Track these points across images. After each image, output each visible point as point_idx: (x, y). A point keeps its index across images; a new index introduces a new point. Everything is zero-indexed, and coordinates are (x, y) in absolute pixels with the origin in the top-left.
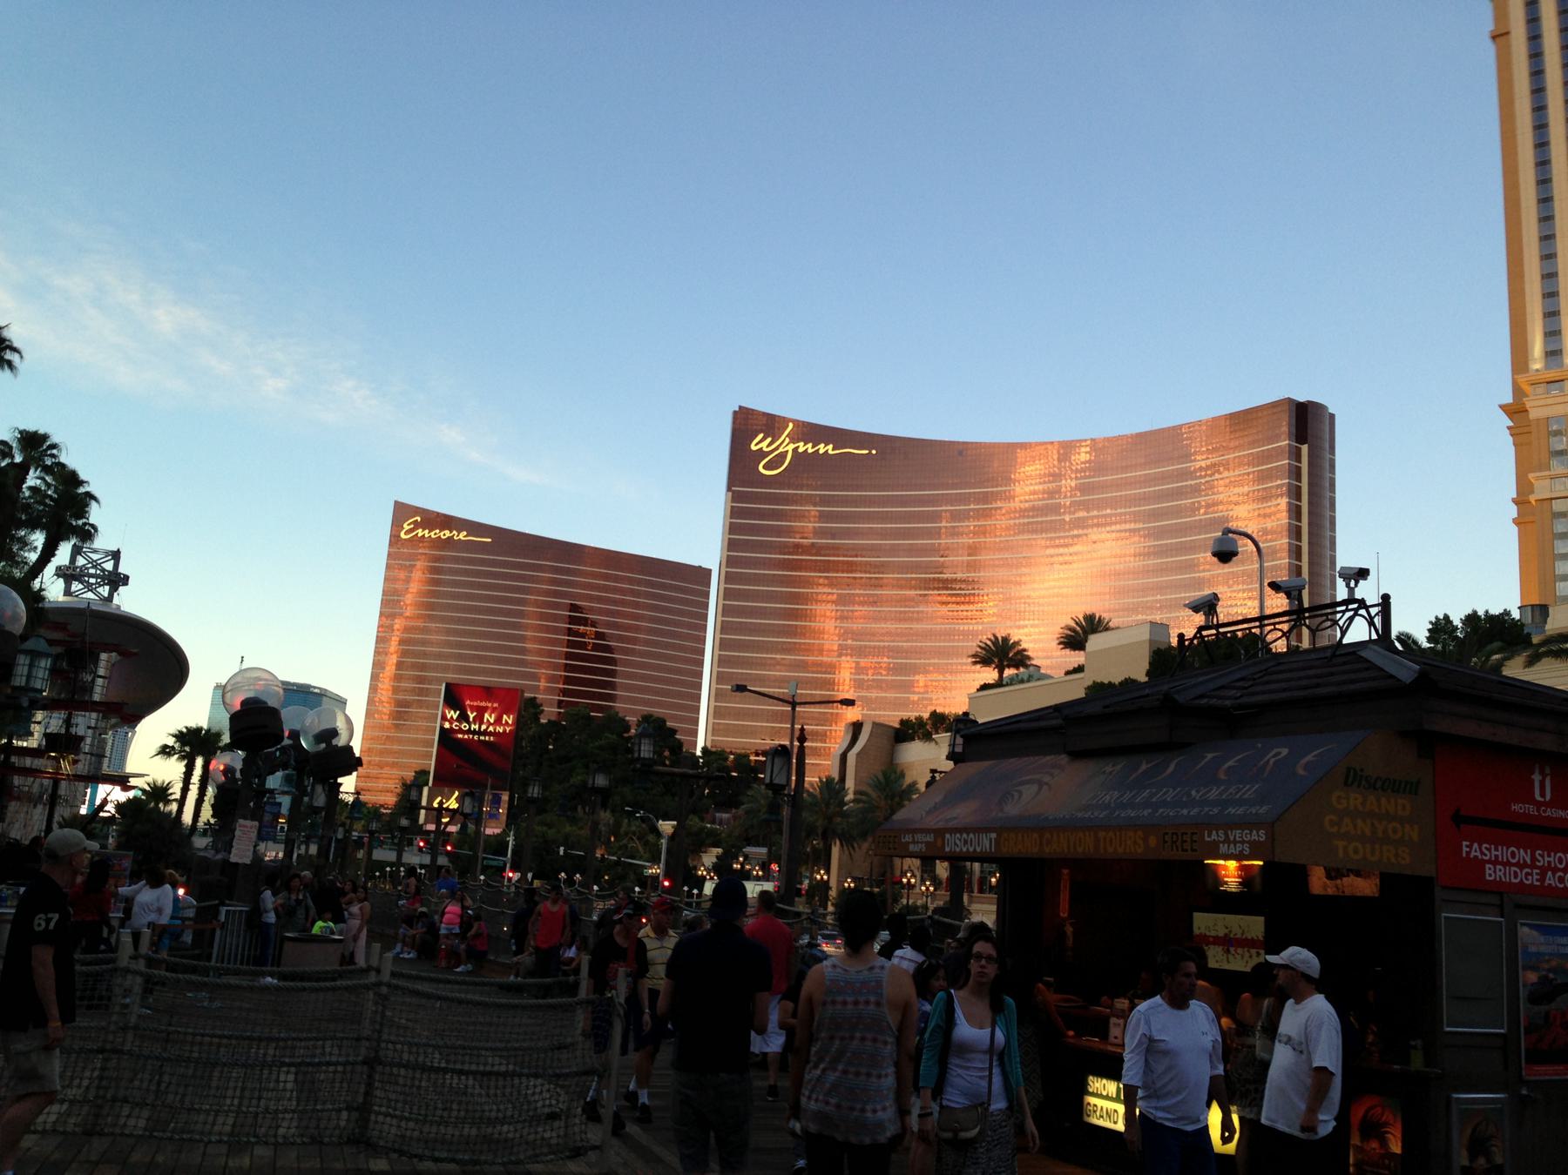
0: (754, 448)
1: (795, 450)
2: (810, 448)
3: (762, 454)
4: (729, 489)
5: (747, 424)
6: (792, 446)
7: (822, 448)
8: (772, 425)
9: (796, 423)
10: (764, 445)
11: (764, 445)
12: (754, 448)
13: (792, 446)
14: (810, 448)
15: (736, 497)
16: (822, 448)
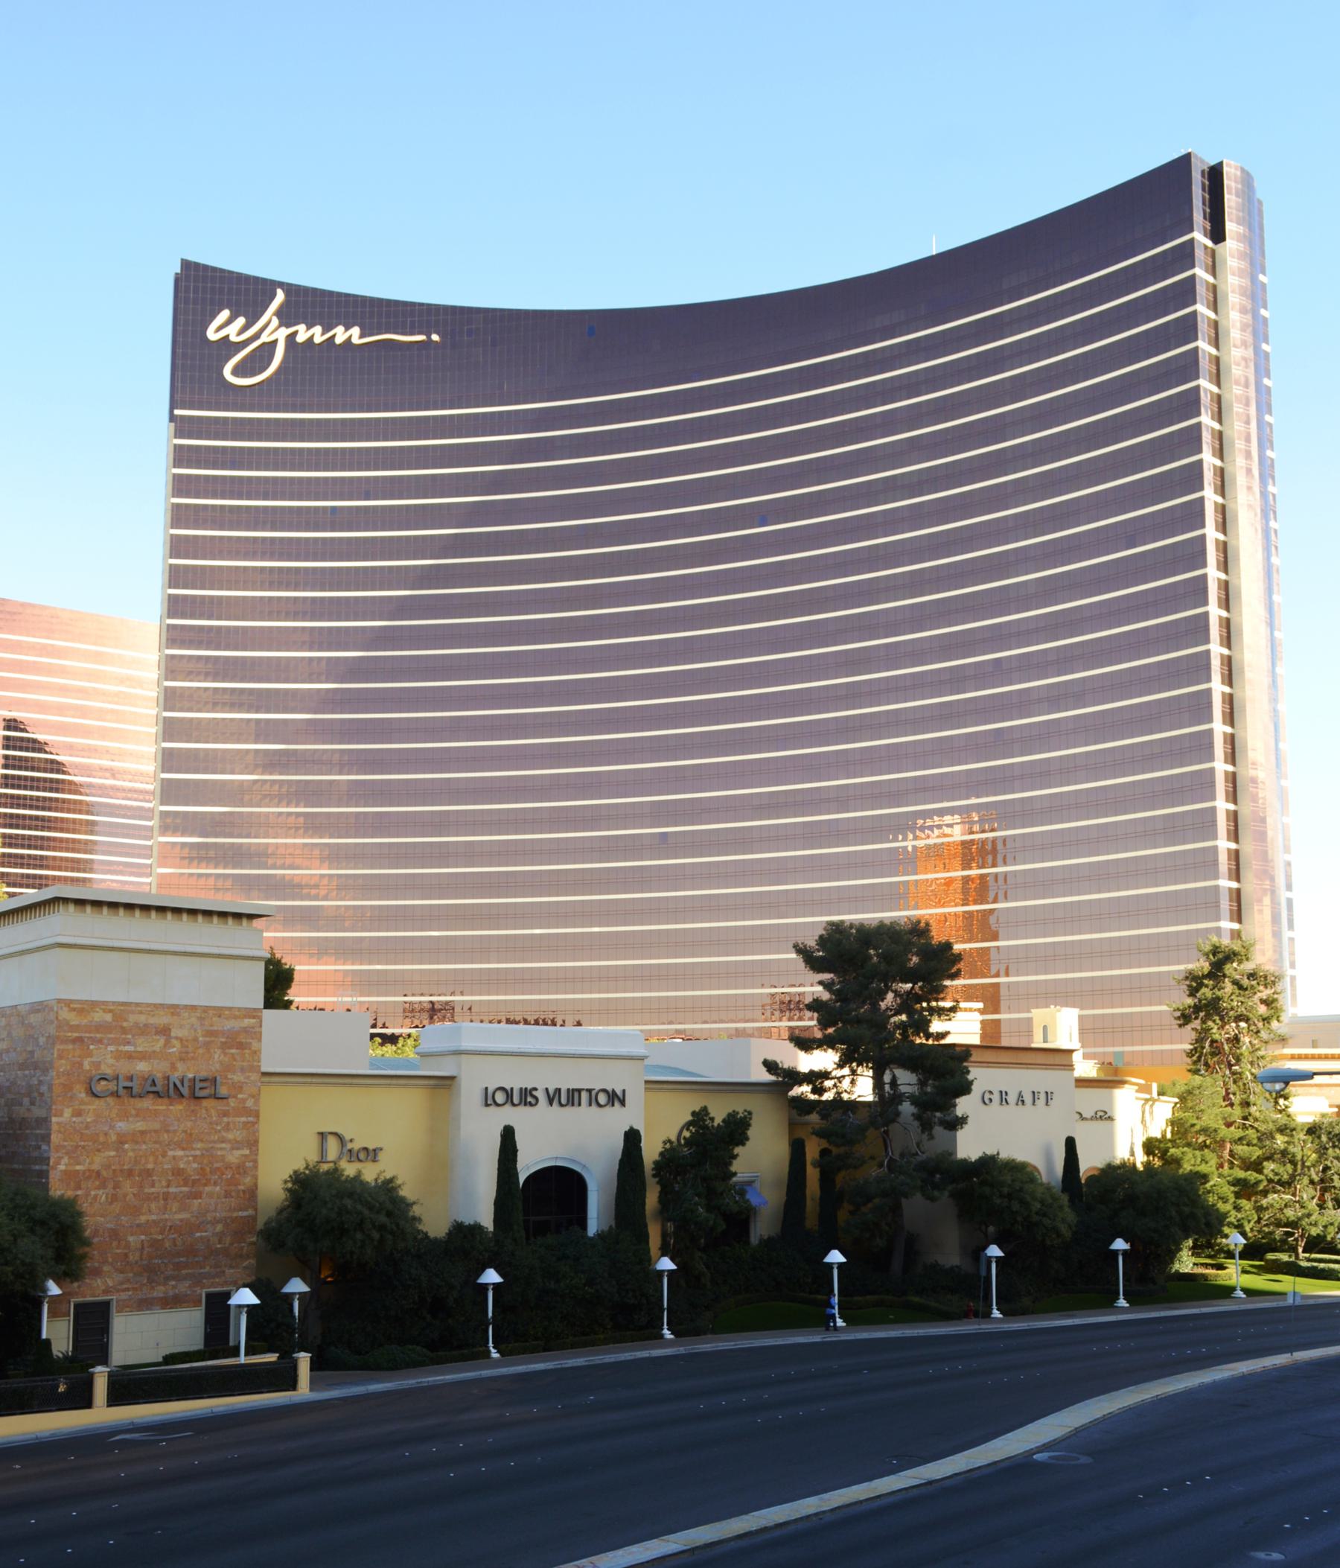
0: (212, 335)
1: (291, 338)
2: (318, 335)
3: (227, 347)
4: (172, 418)
5: (202, 290)
6: (283, 333)
7: (340, 335)
8: (248, 294)
9: (291, 289)
10: (232, 332)
12: (212, 335)
13: (283, 333)
14: (318, 335)
15: (183, 427)
16: (340, 335)
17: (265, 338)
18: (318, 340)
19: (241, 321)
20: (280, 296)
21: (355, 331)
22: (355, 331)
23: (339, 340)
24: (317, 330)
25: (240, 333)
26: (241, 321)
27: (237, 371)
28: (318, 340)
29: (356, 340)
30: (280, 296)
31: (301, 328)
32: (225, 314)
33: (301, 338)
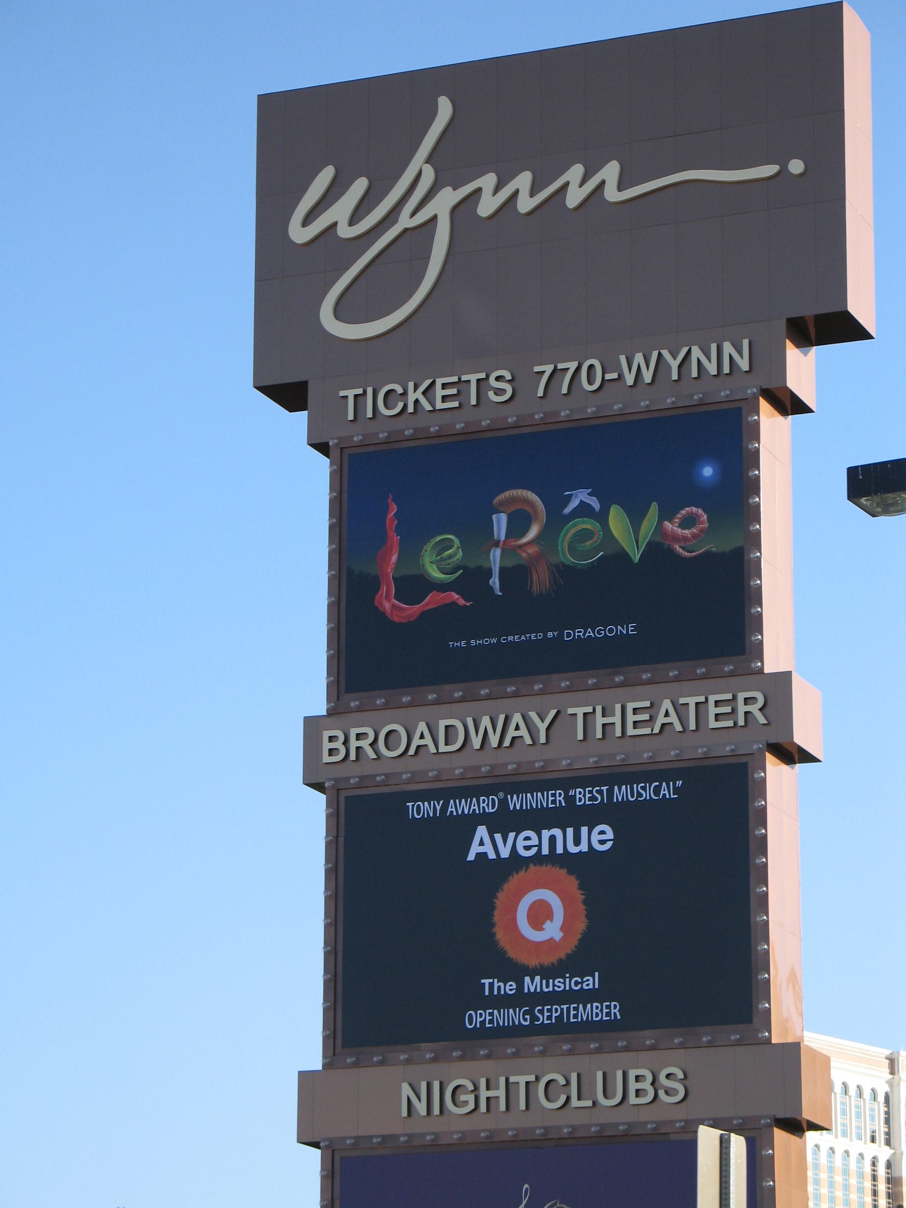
11: (339, 212)
17: (405, 221)
18: (525, 204)
19: (360, 186)
20: (445, 108)
21: (611, 172)
22: (611, 172)
23: (573, 198)
24: (523, 181)
25: (353, 221)
26: (360, 186)
27: (339, 313)
28: (525, 204)
29: (612, 194)
30: (445, 108)
31: (488, 181)
32: (326, 175)
33: (487, 206)
